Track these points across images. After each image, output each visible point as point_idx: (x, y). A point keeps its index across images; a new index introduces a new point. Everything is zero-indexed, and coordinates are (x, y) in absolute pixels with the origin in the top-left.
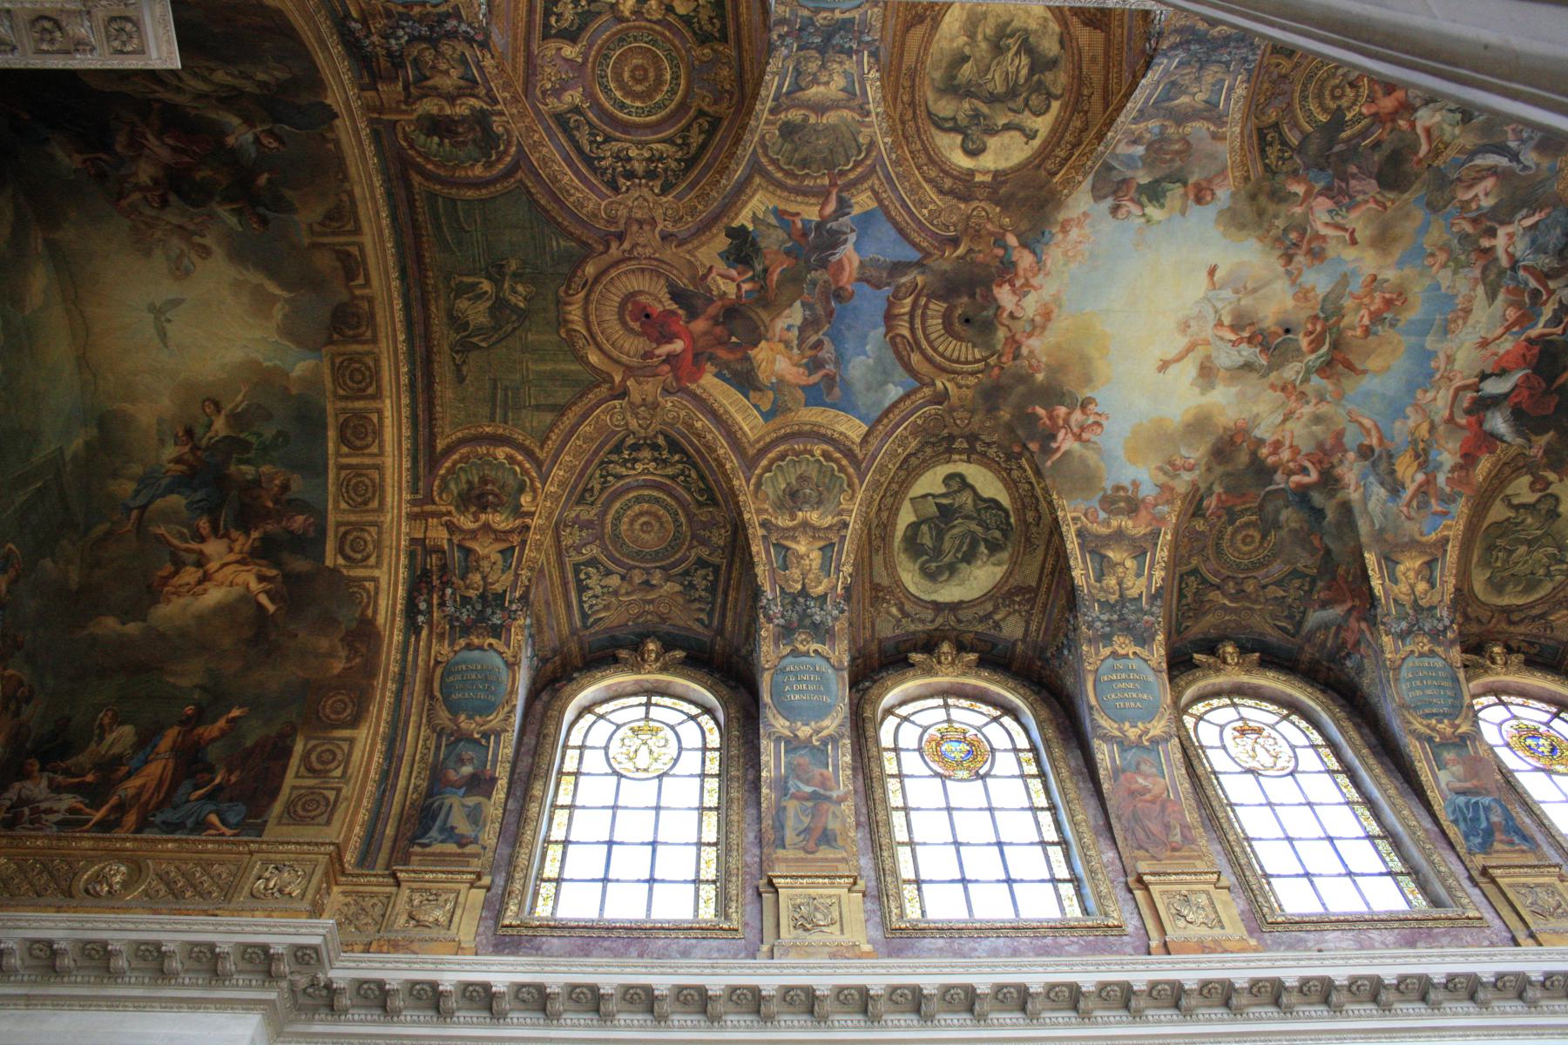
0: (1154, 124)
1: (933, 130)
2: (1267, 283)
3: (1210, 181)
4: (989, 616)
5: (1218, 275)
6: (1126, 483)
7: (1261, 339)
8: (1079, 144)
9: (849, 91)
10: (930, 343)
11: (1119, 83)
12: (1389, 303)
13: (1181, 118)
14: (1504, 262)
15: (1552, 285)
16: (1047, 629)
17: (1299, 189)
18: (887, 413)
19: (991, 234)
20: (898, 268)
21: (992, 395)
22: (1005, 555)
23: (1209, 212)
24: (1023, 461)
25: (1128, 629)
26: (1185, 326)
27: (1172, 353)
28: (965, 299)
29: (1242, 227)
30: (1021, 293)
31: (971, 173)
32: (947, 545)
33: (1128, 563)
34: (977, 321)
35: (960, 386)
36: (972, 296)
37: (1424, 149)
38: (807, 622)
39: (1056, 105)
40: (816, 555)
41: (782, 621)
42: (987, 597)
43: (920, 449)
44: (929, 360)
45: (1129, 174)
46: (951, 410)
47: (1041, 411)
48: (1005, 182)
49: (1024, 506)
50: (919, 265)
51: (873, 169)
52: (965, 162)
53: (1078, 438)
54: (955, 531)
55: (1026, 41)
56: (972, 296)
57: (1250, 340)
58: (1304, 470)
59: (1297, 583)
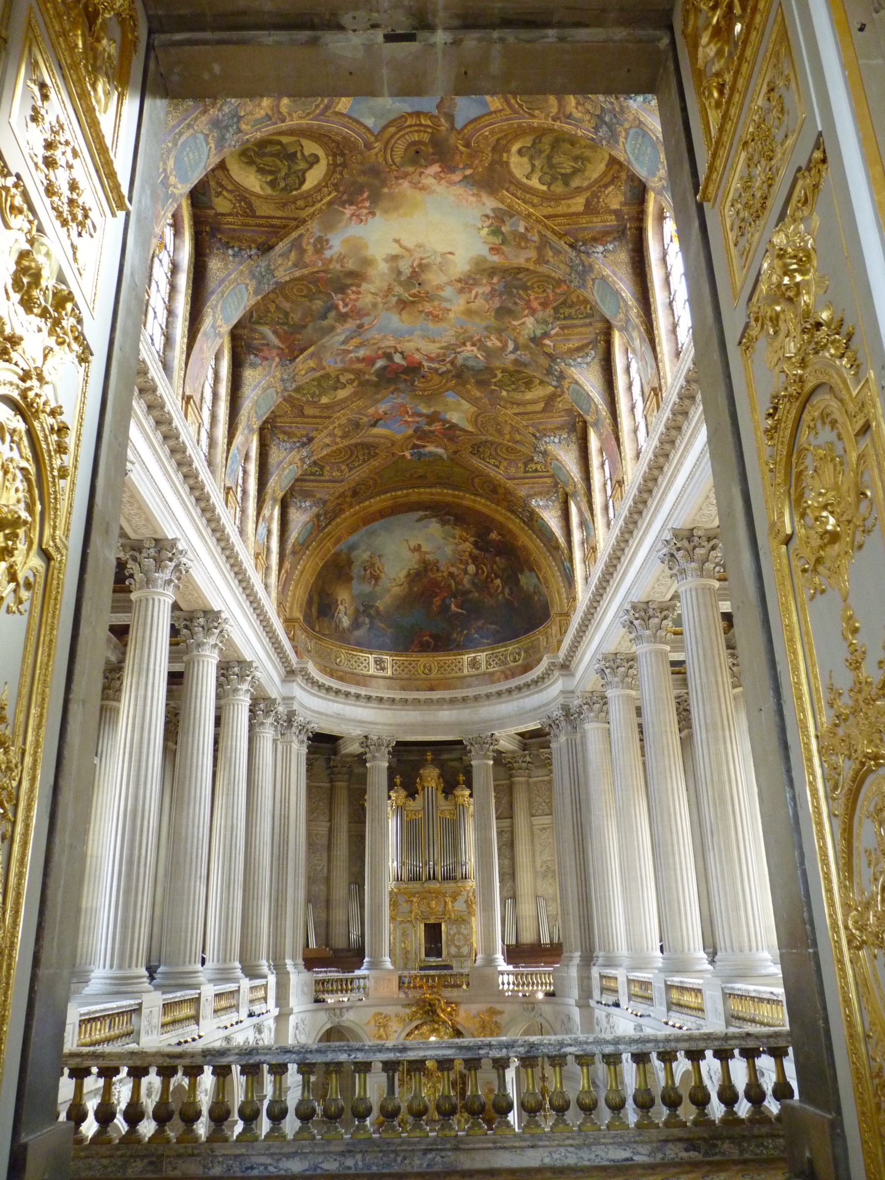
0: (536, 238)
1: (533, 137)
2: (446, 275)
3: (503, 253)
4: (223, 187)
5: (450, 256)
6: (331, 243)
7: (414, 274)
8: (525, 202)
9: (569, 116)
10: (403, 136)
11: (559, 225)
12: (437, 316)
13: (539, 249)
14: (458, 350)
15: (448, 365)
16: (234, 230)
17: (495, 280)
18: (358, 122)
19: (472, 163)
20: (450, 118)
21: (375, 172)
22: (269, 191)
23: (484, 251)
24: (334, 194)
25: (259, 283)
26: (419, 246)
27: (405, 243)
28: (431, 150)
29: (477, 264)
30: (436, 176)
31: (509, 151)
32: (267, 159)
33: (290, 263)
34: (417, 156)
35: (376, 155)
36: (433, 154)
37: (516, 323)
38: (224, 131)
39: (545, 188)
40: (263, 112)
41: (221, 117)
42: (237, 185)
43: (333, 141)
44: (392, 137)
45: (508, 223)
46: (361, 153)
47: (366, 195)
48: (502, 166)
49: (305, 198)
50: (452, 127)
51: (516, 112)
52: (515, 148)
53: (353, 215)
54: (279, 162)
55: (579, 170)
56: (433, 154)
57: (414, 272)
58: (346, 305)
59: (281, 316)
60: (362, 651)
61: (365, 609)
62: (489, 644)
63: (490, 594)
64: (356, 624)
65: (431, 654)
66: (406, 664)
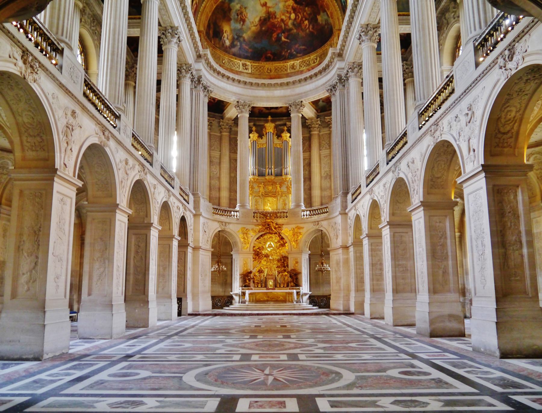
60: (236, 59)
61: (237, 37)
62: (301, 56)
63: (302, 29)
64: (233, 45)
65: (271, 63)
66: (258, 67)
